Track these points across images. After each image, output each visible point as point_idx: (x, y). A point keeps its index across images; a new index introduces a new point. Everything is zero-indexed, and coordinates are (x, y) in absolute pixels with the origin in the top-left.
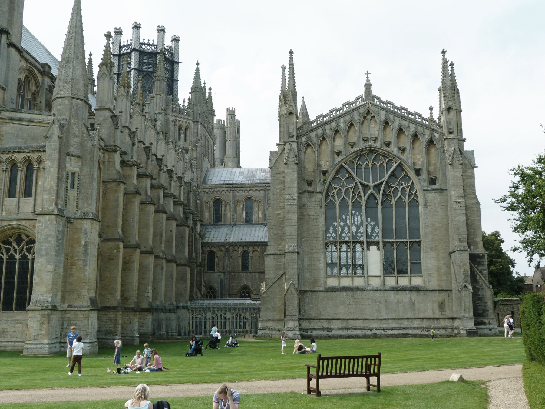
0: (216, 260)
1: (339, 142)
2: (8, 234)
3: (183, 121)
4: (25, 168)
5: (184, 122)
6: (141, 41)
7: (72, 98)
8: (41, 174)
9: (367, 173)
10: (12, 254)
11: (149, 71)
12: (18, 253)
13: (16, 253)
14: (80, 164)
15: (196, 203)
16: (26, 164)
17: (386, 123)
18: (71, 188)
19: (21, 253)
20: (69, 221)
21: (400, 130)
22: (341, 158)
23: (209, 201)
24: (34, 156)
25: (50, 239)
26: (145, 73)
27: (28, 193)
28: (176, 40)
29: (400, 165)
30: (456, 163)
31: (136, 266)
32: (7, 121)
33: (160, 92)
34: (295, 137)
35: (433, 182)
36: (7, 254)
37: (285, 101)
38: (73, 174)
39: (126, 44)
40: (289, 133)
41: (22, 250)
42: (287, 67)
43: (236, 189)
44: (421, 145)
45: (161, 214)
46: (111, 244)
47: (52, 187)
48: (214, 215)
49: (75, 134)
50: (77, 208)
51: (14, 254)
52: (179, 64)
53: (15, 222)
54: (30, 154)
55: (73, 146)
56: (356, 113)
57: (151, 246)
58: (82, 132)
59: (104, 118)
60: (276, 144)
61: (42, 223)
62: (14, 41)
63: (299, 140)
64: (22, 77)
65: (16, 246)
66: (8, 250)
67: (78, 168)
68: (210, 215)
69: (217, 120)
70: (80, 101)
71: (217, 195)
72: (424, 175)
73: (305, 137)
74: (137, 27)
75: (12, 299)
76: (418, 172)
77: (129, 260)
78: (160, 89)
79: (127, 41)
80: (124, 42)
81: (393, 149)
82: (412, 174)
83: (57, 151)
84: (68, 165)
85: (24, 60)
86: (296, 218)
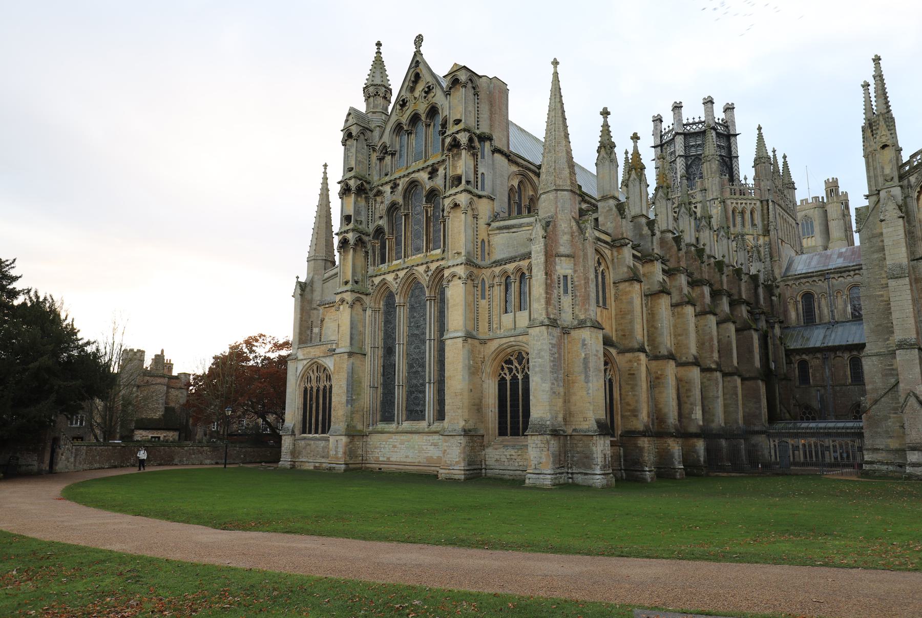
0: (810, 371)
2: (509, 352)
3: (746, 204)
4: (518, 279)
5: (748, 204)
6: (685, 122)
7: (557, 190)
10: (514, 374)
11: (698, 155)
12: (520, 372)
13: (518, 373)
14: (572, 265)
15: (772, 300)
16: (519, 274)
18: (564, 293)
19: (522, 372)
20: (566, 331)
23: (795, 296)
24: (524, 264)
25: (543, 353)
26: (693, 158)
28: (729, 109)
31: (671, 381)
32: (498, 232)
33: (711, 174)
34: (896, 179)
36: (510, 374)
37: (872, 131)
38: (565, 277)
39: (667, 130)
40: (884, 175)
42: (872, 82)
43: (832, 276)
45: (708, 316)
46: (629, 356)
47: (541, 295)
48: (803, 313)
49: (564, 230)
50: (573, 316)
51: (517, 374)
52: (738, 136)
53: (512, 339)
54: (521, 263)
55: (562, 246)
57: (694, 356)
58: (571, 228)
59: (607, 208)
60: (865, 196)
61: (534, 336)
62: (497, 143)
63: (905, 182)
64: (515, 183)
65: (517, 365)
66: (510, 370)
67: (571, 269)
68: (798, 314)
69: (812, 198)
70: (565, 192)
71: (805, 288)
73: (916, 175)
74: (677, 107)
75: (519, 423)
77: (661, 375)
78: (711, 171)
79: (669, 127)
80: (665, 129)
83: (543, 253)
84: (558, 268)
85: (515, 165)
86: (909, 297)
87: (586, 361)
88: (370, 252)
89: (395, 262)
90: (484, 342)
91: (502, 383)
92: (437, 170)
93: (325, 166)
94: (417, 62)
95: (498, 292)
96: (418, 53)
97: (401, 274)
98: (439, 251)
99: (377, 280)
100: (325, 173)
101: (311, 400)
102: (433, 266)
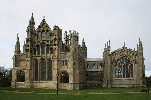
1: (118, 55)
8: (69, 62)
9: (124, 61)
17: (128, 52)
21: (130, 53)
22: (119, 58)
27: (66, 65)
29: (130, 59)
30: (141, 59)
35: (136, 62)
41: (65, 74)
44: (134, 56)
56: (122, 50)
66: (63, 74)
72: (135, 61)
76: (133, 60)
81: (129, 56)
82: (132, 61)
87: (77, 74)
88: (32, 53)
89: (38, 55)
90: (59, 70)
91: (61, 76)
92: (49, 41)
93: (18, 33)
94: (44, 21)
95: (62, 63)
96: (44, 19)
97: (40, 57)
98: (48, 55)
99: (34, 58)
100: (18, 35)
101: (19, 78)
102: (48, 57)
